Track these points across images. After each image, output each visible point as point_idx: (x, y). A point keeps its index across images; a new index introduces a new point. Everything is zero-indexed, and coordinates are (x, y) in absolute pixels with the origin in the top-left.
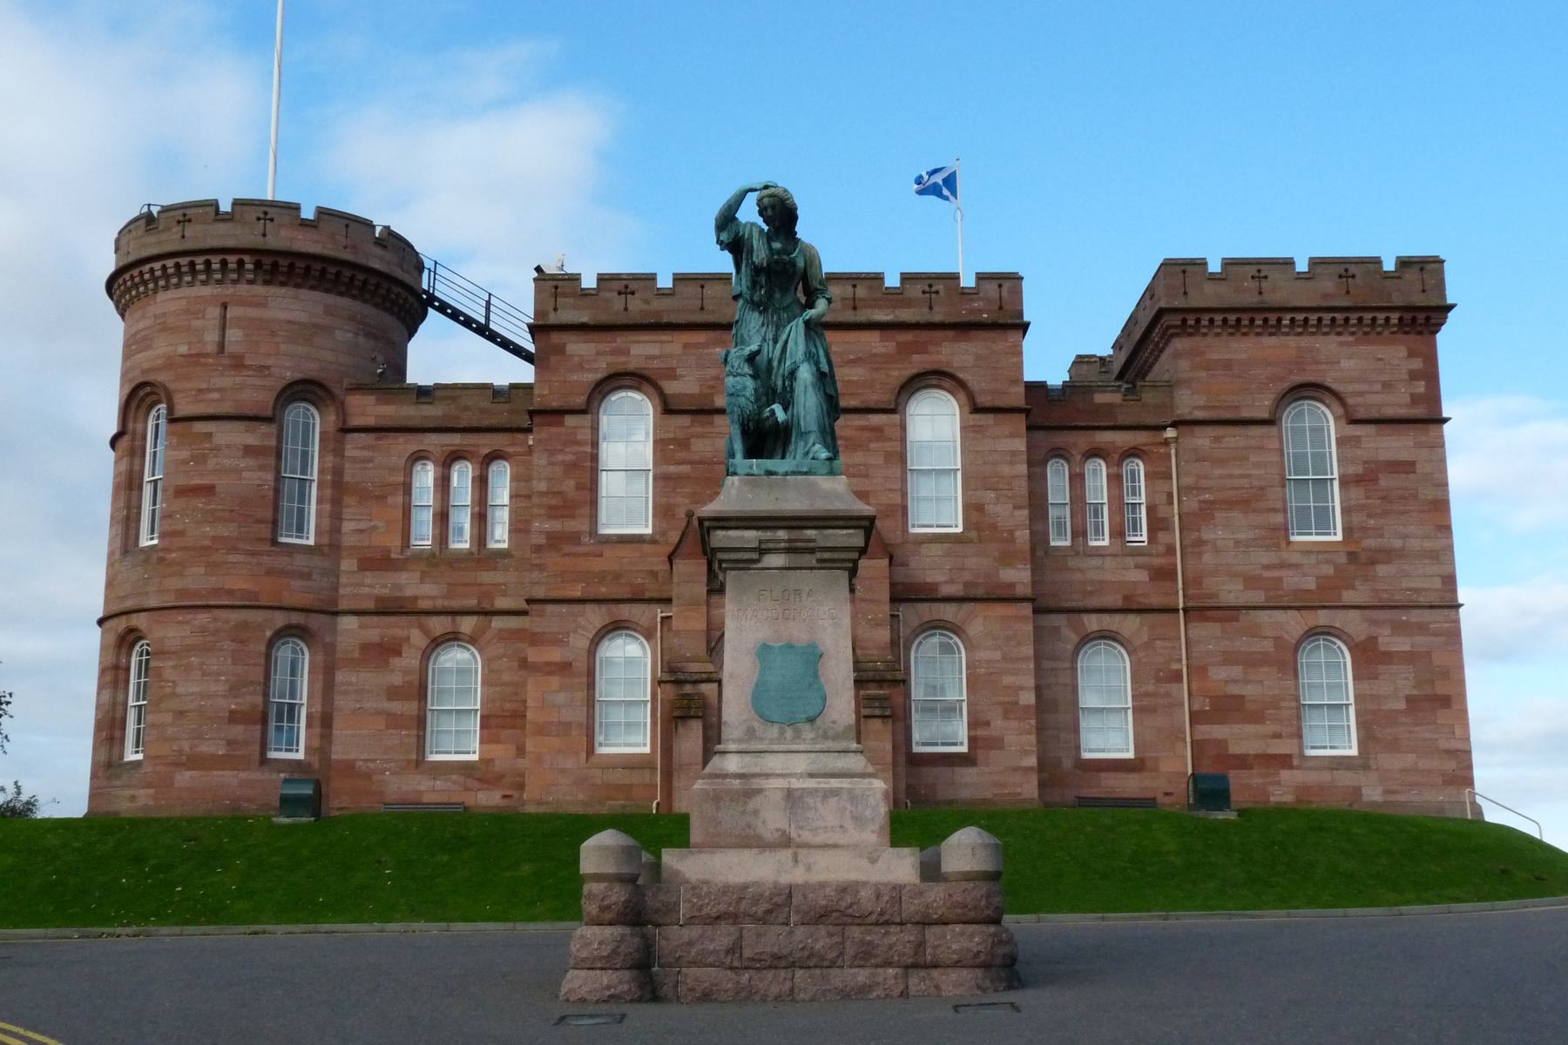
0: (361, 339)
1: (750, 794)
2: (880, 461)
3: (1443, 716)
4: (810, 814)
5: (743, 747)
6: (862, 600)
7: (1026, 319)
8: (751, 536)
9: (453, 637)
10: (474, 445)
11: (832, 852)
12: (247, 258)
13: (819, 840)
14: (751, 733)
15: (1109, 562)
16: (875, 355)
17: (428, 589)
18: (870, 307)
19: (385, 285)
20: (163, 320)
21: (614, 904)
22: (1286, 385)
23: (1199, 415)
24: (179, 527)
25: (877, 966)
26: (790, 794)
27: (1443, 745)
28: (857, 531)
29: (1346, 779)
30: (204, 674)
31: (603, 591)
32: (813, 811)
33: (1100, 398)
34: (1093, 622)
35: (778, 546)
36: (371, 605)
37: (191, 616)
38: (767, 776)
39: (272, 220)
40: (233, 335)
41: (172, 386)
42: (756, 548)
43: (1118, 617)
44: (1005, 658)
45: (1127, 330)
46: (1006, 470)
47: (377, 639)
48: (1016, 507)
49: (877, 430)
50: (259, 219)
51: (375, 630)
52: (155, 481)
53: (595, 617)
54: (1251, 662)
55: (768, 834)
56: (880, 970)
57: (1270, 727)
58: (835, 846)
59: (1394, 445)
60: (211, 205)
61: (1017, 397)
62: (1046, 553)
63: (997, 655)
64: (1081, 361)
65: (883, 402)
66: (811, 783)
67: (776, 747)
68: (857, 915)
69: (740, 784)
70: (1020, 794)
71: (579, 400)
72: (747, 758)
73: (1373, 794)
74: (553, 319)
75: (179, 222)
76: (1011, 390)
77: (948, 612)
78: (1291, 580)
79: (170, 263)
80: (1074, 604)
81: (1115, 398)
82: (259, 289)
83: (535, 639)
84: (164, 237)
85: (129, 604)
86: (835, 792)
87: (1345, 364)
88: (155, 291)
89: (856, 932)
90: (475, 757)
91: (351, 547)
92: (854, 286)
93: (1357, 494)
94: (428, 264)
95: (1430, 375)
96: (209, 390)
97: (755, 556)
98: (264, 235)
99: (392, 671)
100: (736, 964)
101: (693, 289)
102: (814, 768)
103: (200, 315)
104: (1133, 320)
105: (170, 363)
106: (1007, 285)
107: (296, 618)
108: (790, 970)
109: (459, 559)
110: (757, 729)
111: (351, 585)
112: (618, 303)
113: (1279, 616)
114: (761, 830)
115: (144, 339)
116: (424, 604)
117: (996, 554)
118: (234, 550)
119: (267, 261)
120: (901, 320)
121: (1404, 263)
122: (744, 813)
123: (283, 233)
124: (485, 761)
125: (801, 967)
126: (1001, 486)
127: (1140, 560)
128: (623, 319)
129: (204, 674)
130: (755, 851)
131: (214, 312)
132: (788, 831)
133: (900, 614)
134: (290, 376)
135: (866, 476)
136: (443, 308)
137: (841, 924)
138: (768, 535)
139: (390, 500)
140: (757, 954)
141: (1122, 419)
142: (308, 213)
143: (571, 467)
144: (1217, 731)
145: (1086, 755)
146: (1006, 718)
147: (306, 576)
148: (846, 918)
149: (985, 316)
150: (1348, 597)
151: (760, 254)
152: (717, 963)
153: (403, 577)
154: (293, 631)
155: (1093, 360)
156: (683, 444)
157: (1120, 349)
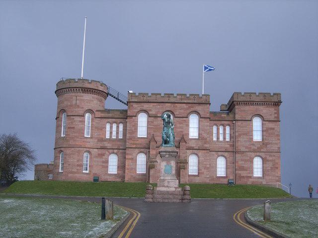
0: (98, 102)
3: (277, 170)
8: (165, 153)
9: (113, 153)
22: (253, 114)
23: (239, 119)
27: (276, 175)
29: (261, 180)
31: (139, 146)
33: (223, 115)
34: (220, 153)
40: (78, 102)
46: (206, 128)
49: (185, 120)
51: (101, 151)
53: (137, 151)
54: (245, 161)
57: (248, 172)
59: (271, 125)
61: (208, 115)
63: (203, 159)
64: (223, 105)
71: (135, 114)
73: (264, 183)
74: (131, 101)
77: (196, 151)
78: (253, 147)
79: (67, 89)
83: (128, 154)
87: (264, 111)
90: (116, 173)
93: (264, 133)
95: (278, 113)
101: (154, 96)
105: (67, 106)
107: (88, 149)
109: (113, 140)
112: (142, 98)
113: (251, 153)
116: (108, 147)
118: (78, 138)
121: (274, 94)
124: (118, 174)
128: (143, 101)
131: (74, 98)
136: (110, 95)
141: (226, 119)
143: (133, 126)
144: (240, 172)
150: (262, 150)
151: (167, 121)
156: (152, 122)
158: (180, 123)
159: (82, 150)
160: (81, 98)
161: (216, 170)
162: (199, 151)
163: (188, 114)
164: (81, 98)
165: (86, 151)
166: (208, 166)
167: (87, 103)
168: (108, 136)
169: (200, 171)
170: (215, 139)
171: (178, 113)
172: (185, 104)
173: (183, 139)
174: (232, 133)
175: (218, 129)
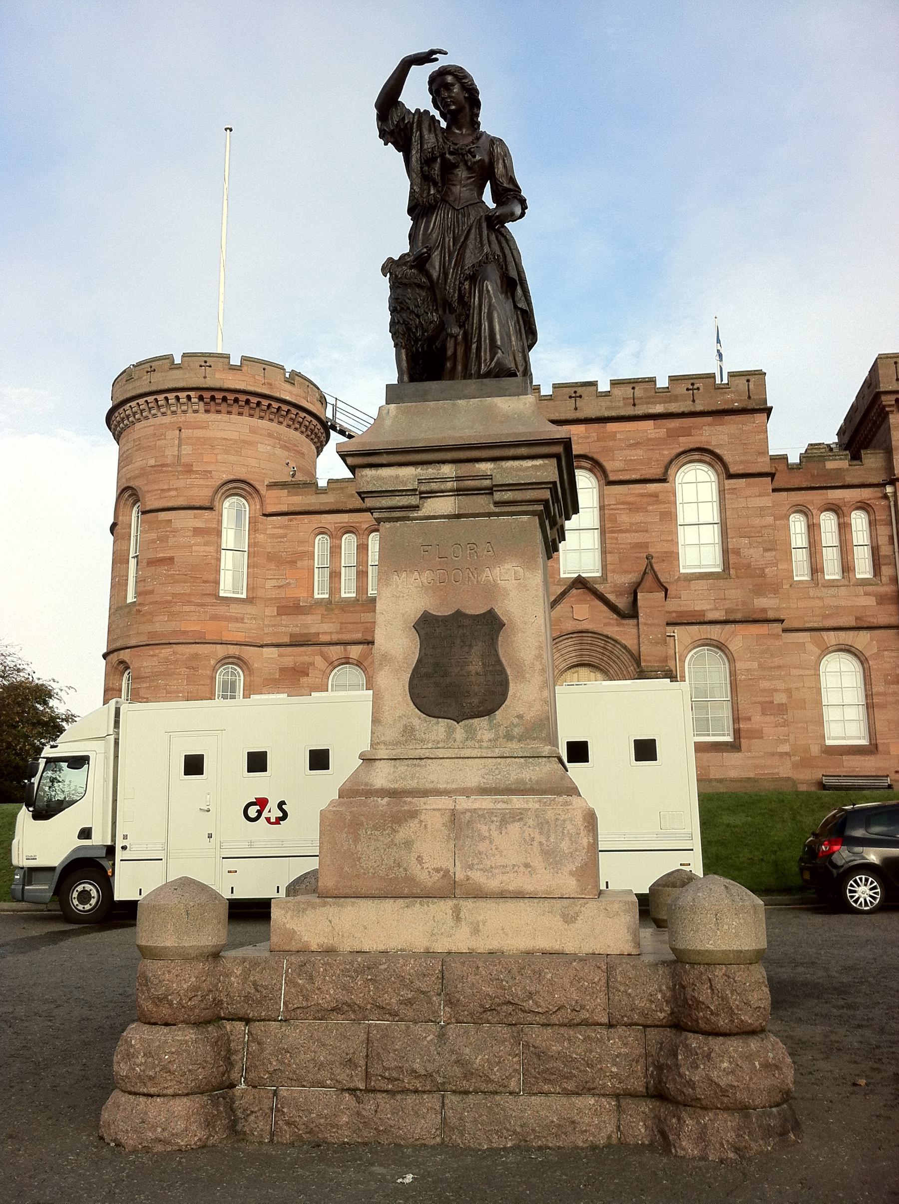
0: (278, 451)
1: (399, 819)
2: (657, 519)
4: (483, 846)
5: (398, 752)
6: (645, 624)
7: (769, 405)
8: (408, 475)
9: (347, 661)
10: (358, 522)
11: (511, 905)
12: (192, 394)
13: (493, 884)
14: (409, 732)
15: (843, 591)
16: (651, 439)
17: (326, 627)
18: (648, 403)
19: (294, 411)
20: (139, 442)
21: (173, 993)
24: (151, 588)
25: (568, 1093)
26: (454, 818)
28: (546, 461)
30: (168, 693)
32: (487, 841)
33: (830, 465)
34: (831, 638)
35: (443, 487)
36: (287, 640)
37: (157, 651)
38: (425, 793)
39: (210, 366)
41: (145, 488)
42: (415, 490)
43: (851, 634)
44: (761, 666)
45: (849, 418)
46: (756, 521)
47: (291, 665)
48: (765, 550)
49: (655, 495)
50: (201, 366)
52: (137, 556)
55: (425, 877)
56: (574, 1099)
58: (519, 896)
60: (168, 358)
62: (791, 586)
63: (755, 665)
65: (656, 474)
66: (485, 803)
67: (440, 753)
68: (540, 1010)
69: (388, 804)
70: (778, 774)
72: (402, 768)
75: (148, 372)
76: (759, 460)
77: (715, 632)
80: (816, 625)
81: (844, 464)
82: (202, 416)
84: (138, 383)
85: (118, 644)
86: (518, 816)
88: (133, 423)
89: (538, 1036)
91: (271, 599)
92: (633, 388)
94: (330, 400)
96: (169, 490)
97: (414, 500)
98: (205, 377)
99: (303, 687)
100: (362, 1086)
102: (490, 781)
103: (163, 437)
104: (854, 409)
106: (753, 379)
107: (233, 650)
108: (436, 1095)
109: (346, 605)
110: (418, 727)
111: (273, 626)
114: (415, 868)
115: (127, 457)
116: (324, 638)
117: (751, 587)
119: (207, 395)
120: (670, 411)
122: (393, 843)
123: (218, 375)
125: (454, 1092)
126: (753, 535)
127: (870, 589)
129: (168, 693)
130: (401, 902)
132: (452, 871)
133: (676, 635)
134: (226, 477)
135: (646, 531)
137: (515, 1025)
138: (430, 471)
139: (299, 564)
140: (389, 1069)
141: (849, 480)
142: (235, 361)
145: (829, 742)
146: (764, 714)
147: (240, 620)
148: (521, 1015)
149: (736, 404)
152: (328, 1082)
153: (309, 619)
154: (230, 660)
155: (822, 447)
157: (844, 434)
158: (633, 508)
159: (208, 657)
160: (199, 433)
161: (821, 716)
162: (728, 627)
163: (667, 468)
164: (199, 433)
165: (226, 660)
166: (780, 698)
167: (227, 452)
168: (320, 594)
169: (742, 726)
170: (801, 572)
171: (618, 465)
172: (651, 423)
173: (649, 578)
174: (883, 541)
175: (813, 529)
